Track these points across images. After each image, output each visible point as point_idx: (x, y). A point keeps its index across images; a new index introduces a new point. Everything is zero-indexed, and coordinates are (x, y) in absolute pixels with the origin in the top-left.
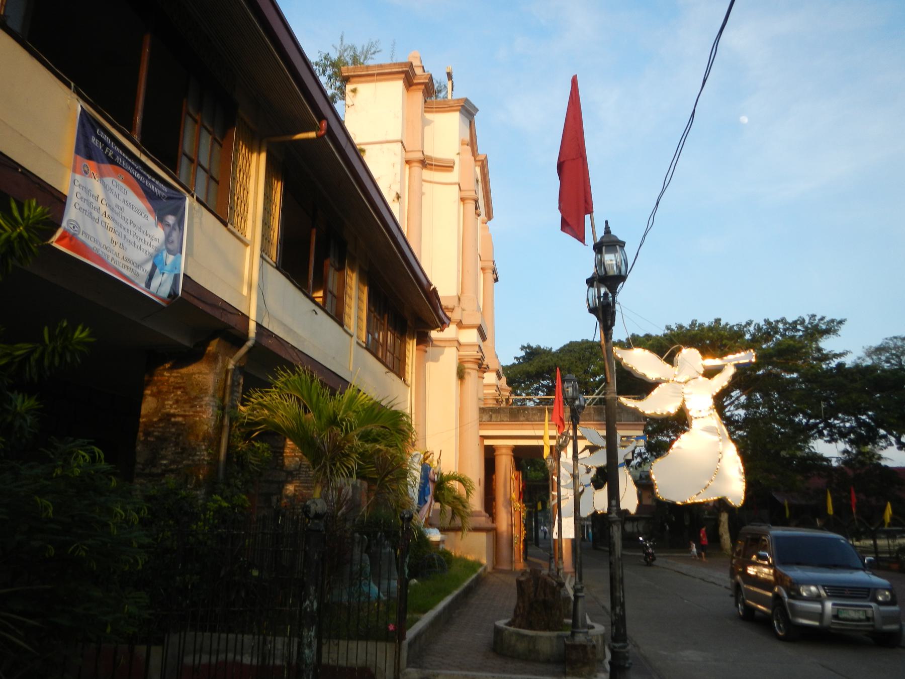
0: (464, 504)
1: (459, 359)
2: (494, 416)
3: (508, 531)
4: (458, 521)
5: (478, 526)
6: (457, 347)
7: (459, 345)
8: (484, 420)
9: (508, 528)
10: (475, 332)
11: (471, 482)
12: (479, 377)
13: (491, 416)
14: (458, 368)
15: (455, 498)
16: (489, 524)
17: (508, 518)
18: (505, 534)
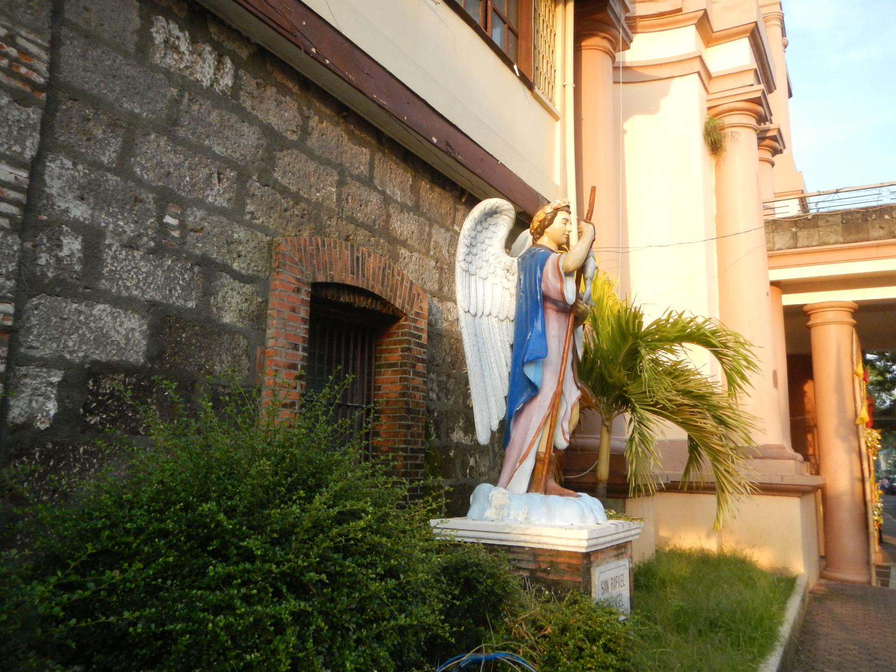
0: (719, 413)
1: (709, 108)
2: (802, 234)
3: (853, 493)
4: (706, 472)
5: (776, 480)
6: (699, 73)
7: (706, 76)
8: (777, 246)
9: (853, 486)
10: (744, 44)
11: (742, 344)
12: (761, 160)
13: (795, 236)
14: (707, 124)
15: (687, 393)
16: (808, 480)
17: (851, 462)
18: (846, 500)
